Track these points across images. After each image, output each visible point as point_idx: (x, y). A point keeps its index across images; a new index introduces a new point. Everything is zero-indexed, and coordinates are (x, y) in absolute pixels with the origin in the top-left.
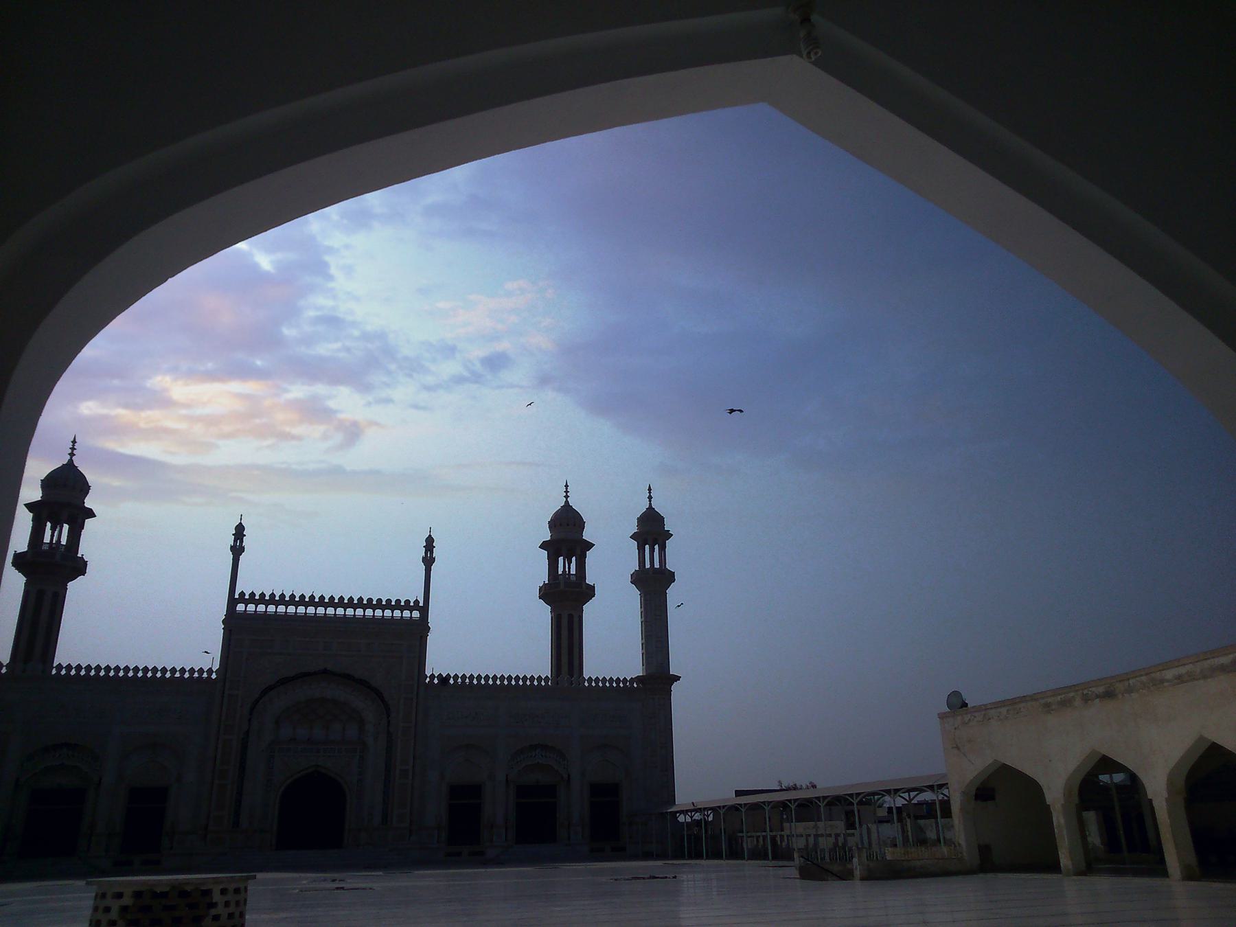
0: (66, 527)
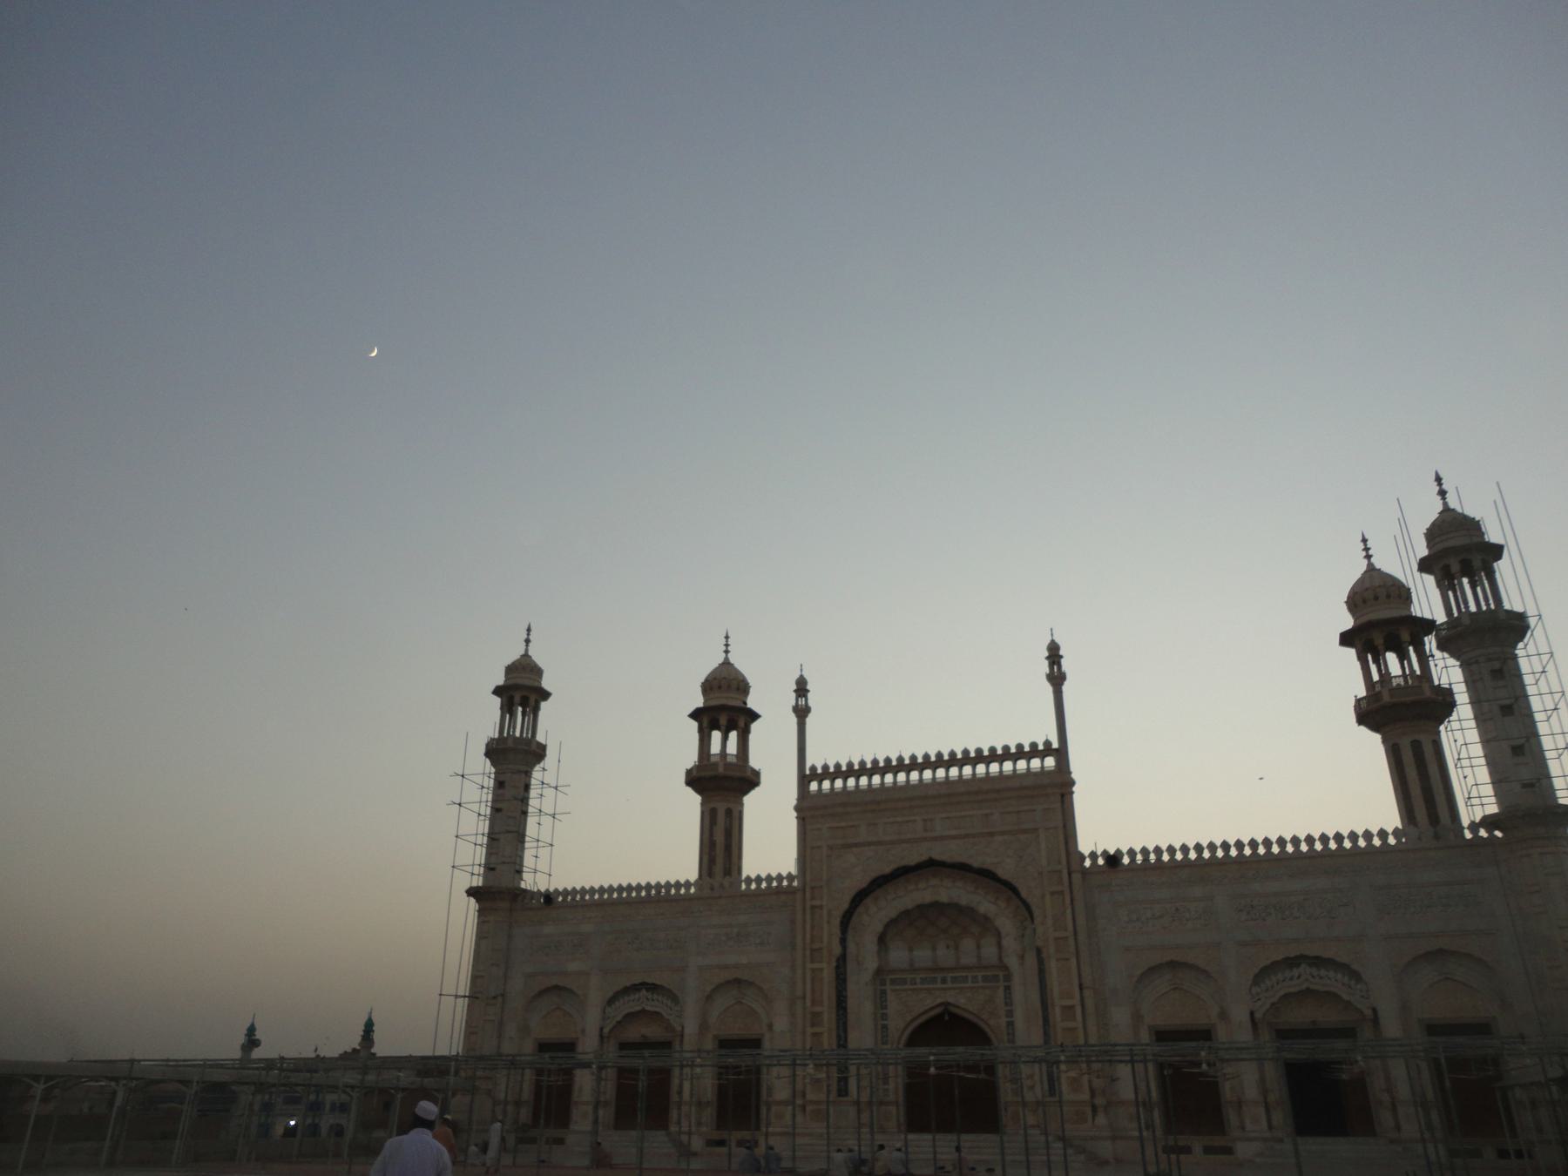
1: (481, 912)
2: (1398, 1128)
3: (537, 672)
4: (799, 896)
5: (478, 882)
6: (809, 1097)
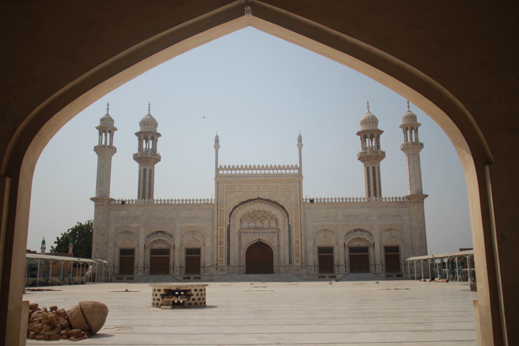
0: (151, 141)
1: (96, 206)
2: (375, 271)
3: (113, 121)
4: (216, 206)
5: (94, 195)
6: (218, 265)
